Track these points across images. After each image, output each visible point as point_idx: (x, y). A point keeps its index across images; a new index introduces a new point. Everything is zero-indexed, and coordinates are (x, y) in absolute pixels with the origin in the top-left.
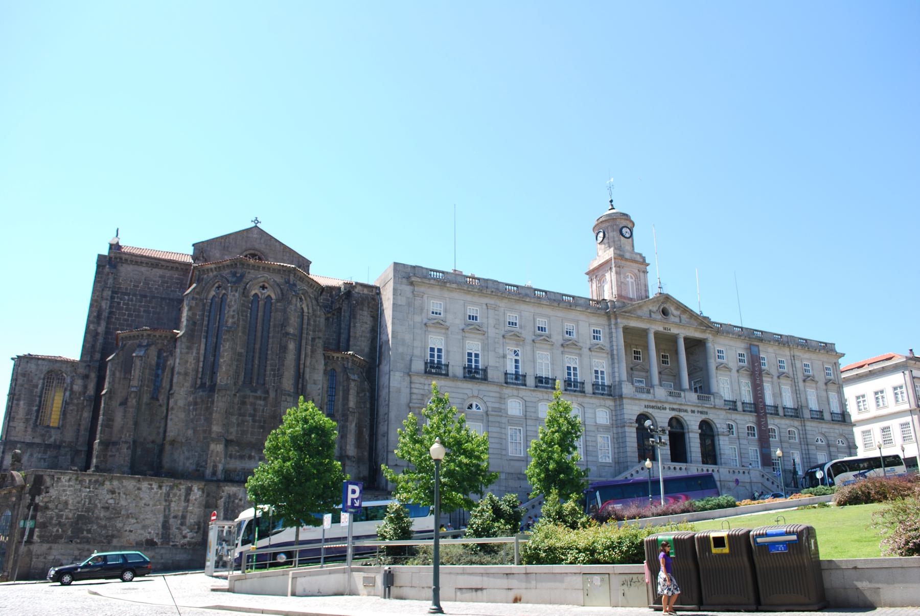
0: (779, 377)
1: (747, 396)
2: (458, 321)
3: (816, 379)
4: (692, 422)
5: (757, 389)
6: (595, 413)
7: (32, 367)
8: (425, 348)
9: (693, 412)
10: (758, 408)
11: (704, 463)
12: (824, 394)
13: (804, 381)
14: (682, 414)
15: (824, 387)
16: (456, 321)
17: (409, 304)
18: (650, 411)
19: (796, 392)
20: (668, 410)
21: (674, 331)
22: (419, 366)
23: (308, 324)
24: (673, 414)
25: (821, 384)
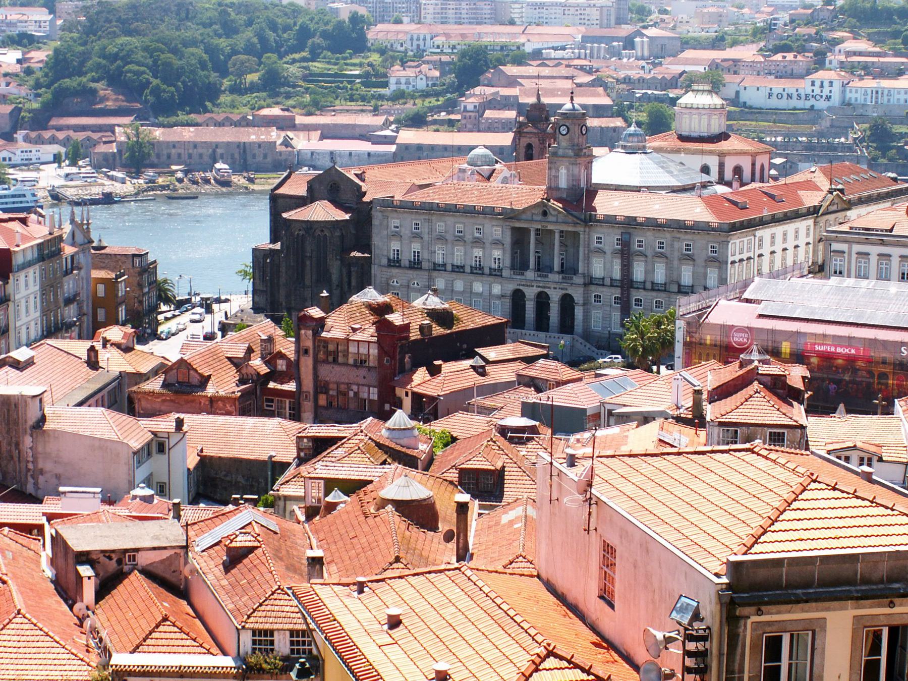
0: (653, 256)
1: (617, 274)
2: (407, 232)
3: (695, 258)
4: (555, 296)
5: (627, 268)
6: (490, 287)
7: (258, 253)
8: (388, 251)
9: (555, 288)
10: (627, 283)
11: (537, 330)
12: (702, 270)
13: (680, 259)
14: (546, 290)
15: (704, 264)
16: (406, 232)
17: (381, 224)
18: (521, 288)
19: (669, 268)
20: (535, 288)
21: (550, 227)
22: (385, 261)
23: (330, 242)
24: (540, 290)
25: (700, 261)
